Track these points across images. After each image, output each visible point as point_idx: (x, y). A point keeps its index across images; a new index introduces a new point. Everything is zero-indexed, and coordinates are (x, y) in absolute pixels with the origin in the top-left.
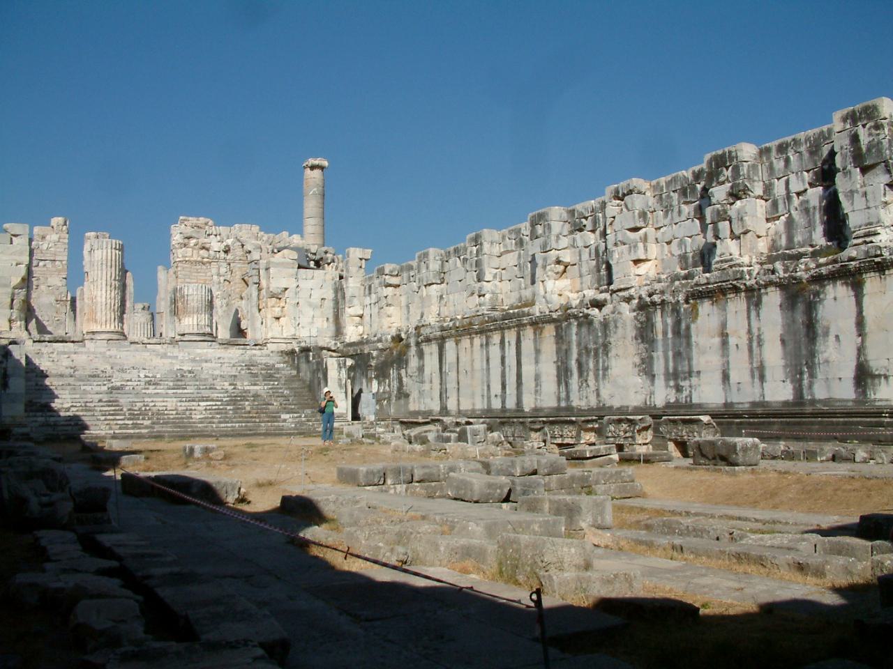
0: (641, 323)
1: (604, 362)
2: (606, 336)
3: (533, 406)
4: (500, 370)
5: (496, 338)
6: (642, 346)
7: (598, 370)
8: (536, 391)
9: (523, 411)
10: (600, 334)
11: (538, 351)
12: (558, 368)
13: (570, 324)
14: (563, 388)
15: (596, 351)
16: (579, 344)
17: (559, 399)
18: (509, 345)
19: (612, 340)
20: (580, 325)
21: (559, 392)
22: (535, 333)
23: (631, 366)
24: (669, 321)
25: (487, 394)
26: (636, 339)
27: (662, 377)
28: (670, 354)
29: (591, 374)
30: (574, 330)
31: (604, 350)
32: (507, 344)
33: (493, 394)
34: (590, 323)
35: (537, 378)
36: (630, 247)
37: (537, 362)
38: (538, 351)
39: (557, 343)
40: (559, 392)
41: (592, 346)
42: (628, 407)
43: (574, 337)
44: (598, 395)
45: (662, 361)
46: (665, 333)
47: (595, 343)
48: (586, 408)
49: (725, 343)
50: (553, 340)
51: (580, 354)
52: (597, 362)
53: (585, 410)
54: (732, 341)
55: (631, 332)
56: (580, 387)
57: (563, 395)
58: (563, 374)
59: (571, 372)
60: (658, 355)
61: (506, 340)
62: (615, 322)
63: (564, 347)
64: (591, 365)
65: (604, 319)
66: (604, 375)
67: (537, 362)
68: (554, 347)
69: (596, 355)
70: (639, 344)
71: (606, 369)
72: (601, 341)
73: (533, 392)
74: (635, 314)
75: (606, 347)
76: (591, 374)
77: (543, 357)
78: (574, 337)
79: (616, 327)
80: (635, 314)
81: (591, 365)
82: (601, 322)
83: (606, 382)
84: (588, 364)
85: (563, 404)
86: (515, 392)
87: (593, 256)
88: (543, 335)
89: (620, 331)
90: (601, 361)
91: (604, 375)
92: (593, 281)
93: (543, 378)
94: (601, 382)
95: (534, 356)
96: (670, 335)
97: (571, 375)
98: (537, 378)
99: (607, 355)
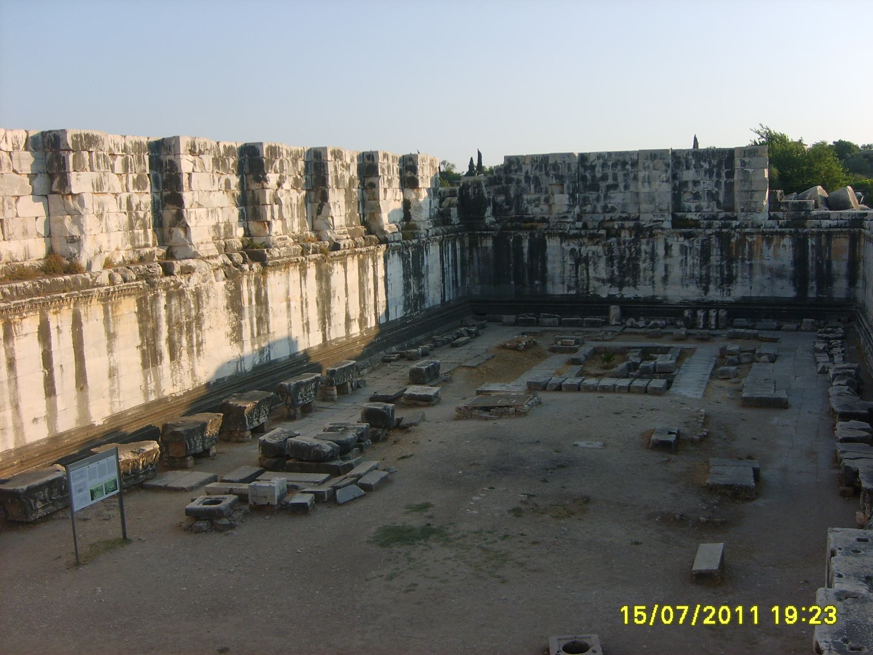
0: (231, 292)
1: (198, 336)
2: (198, 307)
3: (108, 414)
4: (42, 375)
5: (30, 324)
6: (232, 314)
7: (192, 346)
8: (112, 392)
9: (92, 426)
10: (192, 306)
11: (111, 336)
12: (144, 354)
13: (156, 296)
14: (151, 379)
15: (189, 325)
16: (169, 321)
17: (146, 393)
18: (59, 330)
19: (204, 311)
20: (169, 297)
21: (146, 384)
22: (106, 312)
23: (224, 336)
24: (253, 289)
25: (14, 421)
26: (228, 308)
27: (249, 343)
28: (255, 320)
29: (184, 352)
30: (163, 301)
31: (198, 323)
32: (53, 332)
33: (26, 418)
34: (181, 293)
35: (113, 373)
36: (208, 211)
37: (110, 350)
38: (111, 336)
39: (140, 321)
40: (146, 384)
41: (184, 320)
42: (223, 379)
43: (163, 313)
44: (193, 374)
45: (249, 327)
46: (250, 301)
47: (188, 316)
48: (182, 393)
49: (289, 306)
50: (134, 318)
51: (171, 333)
52: (191, 337)
53: (181, 396)
54: (293, 304)
55: (223, 302)
56: (172, 371)
57: (152, 386)
58: (150, 358)
59: (161, 355)
60: (246, 322)
61: (53, 326)
62: (207, 291)
63: (150, 325)
64: (184, 342)
65: (196, 288)
66: (199, 351)
67: (110, 350)
68: (136, 327)
69: (189, 331)
70: (230, 313)
71: (200, 344)
72: (193, 313)
73: (107, 393)
74: (225, 283)
75: (199, 319)
76: (184, 352)
77: (119, 343)
78: (163, 313)
79: (208, 297)
80: (225, 283)
81: (184, 342)
82: (192, 292)
83: (201, 358)
84: (180, 342)
85: (152, 398)
86: (75, 403)
87: (125, 208)
88: (119, 313)
89: (212, 301)
90: (194, 336)
91: (199, 351)
92: (125, 240)
93: (123, 371)
94: (196, 360)
95: (105, 342)
96: (254, 303)
97: (161, 358)
98: (113, 373)
99: (200, 328)
